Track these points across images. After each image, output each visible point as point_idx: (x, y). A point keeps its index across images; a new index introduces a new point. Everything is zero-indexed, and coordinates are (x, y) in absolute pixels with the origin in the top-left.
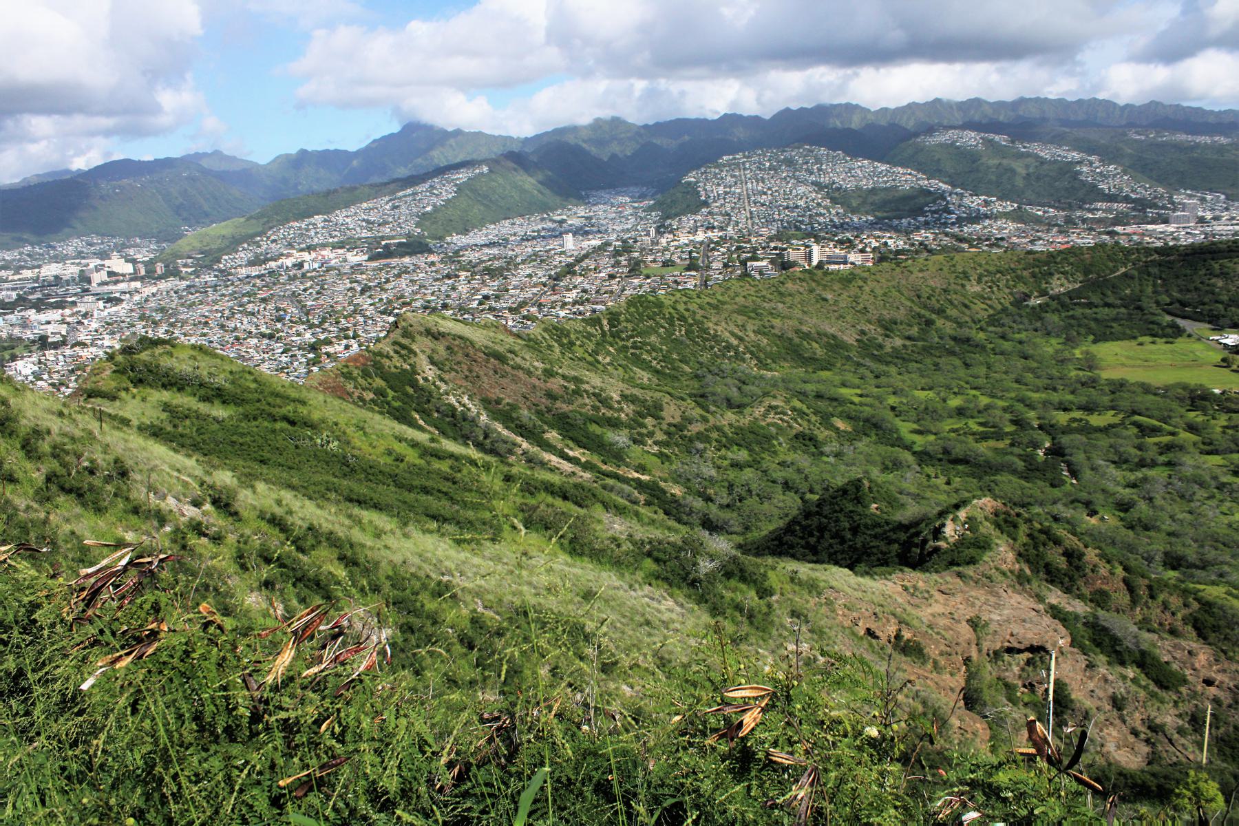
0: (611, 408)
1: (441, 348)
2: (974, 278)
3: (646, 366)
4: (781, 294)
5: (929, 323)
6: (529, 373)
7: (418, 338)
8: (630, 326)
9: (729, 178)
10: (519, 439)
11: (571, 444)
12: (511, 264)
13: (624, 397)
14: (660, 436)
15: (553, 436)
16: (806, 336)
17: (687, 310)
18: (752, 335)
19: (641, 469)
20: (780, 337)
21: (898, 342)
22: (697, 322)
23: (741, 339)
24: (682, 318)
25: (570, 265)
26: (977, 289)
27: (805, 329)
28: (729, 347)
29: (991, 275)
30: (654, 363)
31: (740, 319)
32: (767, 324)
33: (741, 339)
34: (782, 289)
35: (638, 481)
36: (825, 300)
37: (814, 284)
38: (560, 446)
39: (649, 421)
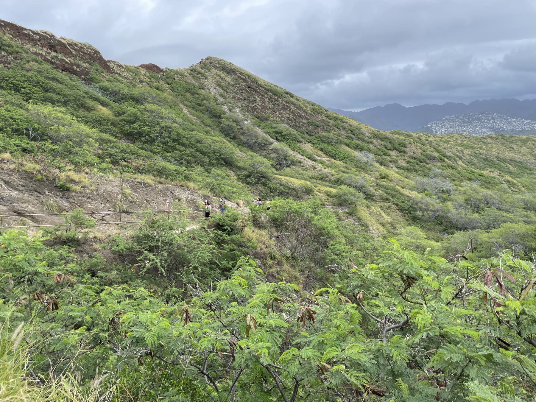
0: (362, 140)
1: (229, 79)
6: (299, 108)
7: (214, 70)
9: (447, 125)
11: (320, 153)
13: (376, 136)
14: (402, 163)
15: (308, 147)
17: (427, 140)
18: (467, 156)
20: (486, 160)
31: (459, 148)
32: (477, 152)
34: (486, 141)
36: (513, 148)
37: (504, 141)
39: (394, 153)
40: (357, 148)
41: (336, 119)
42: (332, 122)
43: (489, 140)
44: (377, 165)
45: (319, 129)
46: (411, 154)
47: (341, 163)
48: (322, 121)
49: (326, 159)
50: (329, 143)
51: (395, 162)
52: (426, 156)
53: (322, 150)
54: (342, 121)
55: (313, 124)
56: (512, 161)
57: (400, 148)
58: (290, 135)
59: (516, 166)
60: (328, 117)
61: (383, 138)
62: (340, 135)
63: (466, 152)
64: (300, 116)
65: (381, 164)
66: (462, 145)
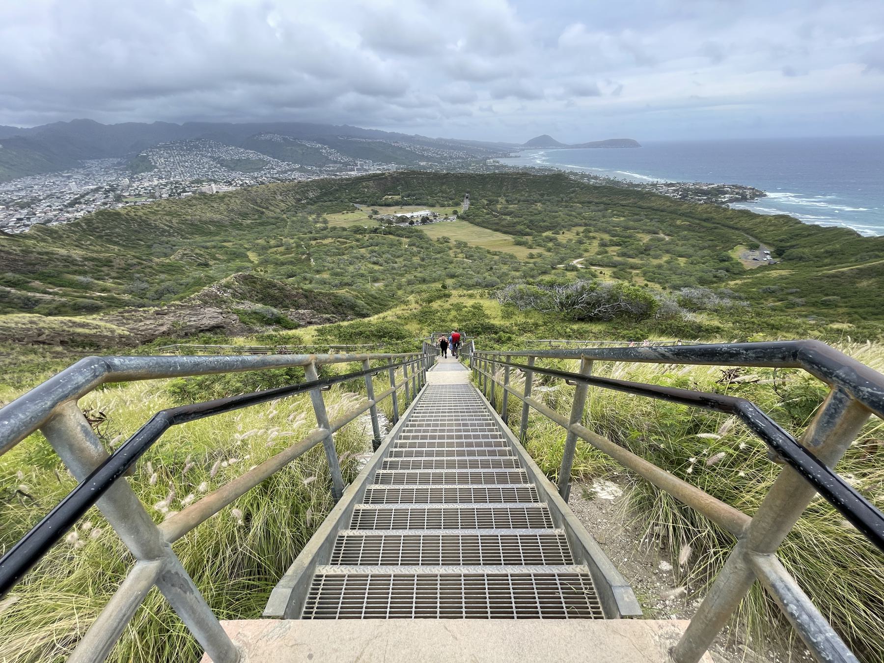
2: (278, 193)
3: (116, 243)
4: (190, 206)
5: (263, 213)
6: (9, 253)
8: (100, 225)
10: (8, 289)
11: (50, 286)
12: (36, 201)
13: (86, 259)
14: (114, 274)
15: (37, 284)
16: (206, 223)
19: (103, 290)
20: (192, 224)
21: (249, 222)
22: (144, 221)
23: (171, 227)
24: (133, 219)
25: (76, 199)
26: (280, 198)
27: (204, 219)
28: (164, 231)
29: (285, 193)
30: (121, 242)
31: (168, 218)
33: (171, 227)
34: (190, 203)
35: (101, 297)
38: (42, 288)
39: (105, 269)
40: (75, 272)
41: (47, 253)
42: (45, 257)
43: (194, 201)
44: (96, 281)
45: (37, 266)
46: (118, 266)
47: (70, 289)
48: (36, 259)
49: (56, 290)
50: (52, 277)
51: (108, 275)
52: (128, 265)
53: (50, 283)
54: (52, 254)
55: (31, 264)
56: (212, 222)
57: (108, 263)
58: (19, 281)
59: (214, 226)
60: (39, 253)
61: (93, 259)
62: (56, 266)
63: (174, 221)
64: (15, 260)
65: (98, 279)
66: (169, 214)
